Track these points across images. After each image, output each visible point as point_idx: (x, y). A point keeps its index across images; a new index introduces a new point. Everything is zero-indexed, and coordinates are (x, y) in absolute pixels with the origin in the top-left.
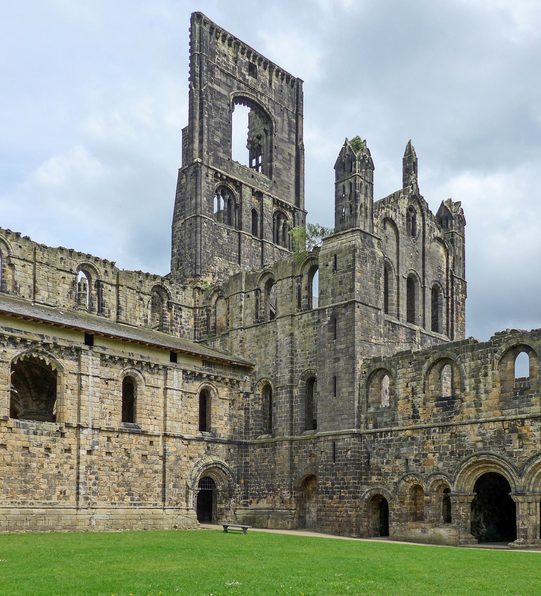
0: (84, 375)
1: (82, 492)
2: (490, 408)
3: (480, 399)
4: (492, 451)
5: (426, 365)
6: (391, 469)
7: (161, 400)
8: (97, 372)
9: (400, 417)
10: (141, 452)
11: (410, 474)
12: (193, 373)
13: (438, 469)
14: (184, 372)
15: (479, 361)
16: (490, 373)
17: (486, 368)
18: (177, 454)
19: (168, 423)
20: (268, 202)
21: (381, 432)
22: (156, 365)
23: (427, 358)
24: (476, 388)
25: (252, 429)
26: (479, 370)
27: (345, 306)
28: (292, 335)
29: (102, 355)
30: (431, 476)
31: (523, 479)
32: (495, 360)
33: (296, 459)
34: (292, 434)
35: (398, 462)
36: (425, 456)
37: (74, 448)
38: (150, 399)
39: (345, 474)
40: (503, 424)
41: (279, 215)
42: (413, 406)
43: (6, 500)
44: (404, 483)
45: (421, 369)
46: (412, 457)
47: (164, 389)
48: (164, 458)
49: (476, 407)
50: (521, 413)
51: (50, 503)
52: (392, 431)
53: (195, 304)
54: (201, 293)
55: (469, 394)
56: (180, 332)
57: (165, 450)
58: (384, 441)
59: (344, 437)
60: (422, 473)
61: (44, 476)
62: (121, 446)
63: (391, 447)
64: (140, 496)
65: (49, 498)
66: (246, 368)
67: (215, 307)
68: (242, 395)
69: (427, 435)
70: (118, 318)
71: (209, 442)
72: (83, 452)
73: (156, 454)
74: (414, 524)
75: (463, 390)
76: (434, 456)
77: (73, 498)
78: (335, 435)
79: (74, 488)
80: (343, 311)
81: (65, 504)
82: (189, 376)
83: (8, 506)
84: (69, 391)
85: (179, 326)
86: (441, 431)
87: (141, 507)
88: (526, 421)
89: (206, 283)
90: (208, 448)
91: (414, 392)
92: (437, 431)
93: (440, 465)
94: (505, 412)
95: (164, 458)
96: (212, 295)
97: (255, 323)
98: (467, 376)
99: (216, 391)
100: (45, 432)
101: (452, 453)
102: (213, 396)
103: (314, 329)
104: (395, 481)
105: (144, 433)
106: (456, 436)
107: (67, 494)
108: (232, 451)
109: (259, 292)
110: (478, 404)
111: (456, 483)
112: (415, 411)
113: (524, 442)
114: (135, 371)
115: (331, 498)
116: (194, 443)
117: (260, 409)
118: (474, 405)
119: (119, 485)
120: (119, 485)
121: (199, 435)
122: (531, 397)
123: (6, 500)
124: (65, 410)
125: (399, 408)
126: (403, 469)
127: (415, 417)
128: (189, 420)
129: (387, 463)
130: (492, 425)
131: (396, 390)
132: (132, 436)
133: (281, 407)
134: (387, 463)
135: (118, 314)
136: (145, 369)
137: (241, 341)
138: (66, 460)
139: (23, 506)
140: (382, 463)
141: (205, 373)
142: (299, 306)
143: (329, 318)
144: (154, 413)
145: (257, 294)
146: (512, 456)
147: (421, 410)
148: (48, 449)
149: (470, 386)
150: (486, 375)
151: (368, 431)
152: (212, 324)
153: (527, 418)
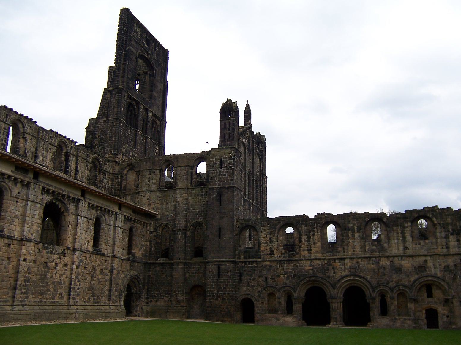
0: (79, 216)
1: (72, 294)
2: (317, 252)
3: (311, 247)
4: (318, 275)
5: (278, 226)
6: (256, 283)
7: (111, 234)
8: (86, 215)
9: (261, 253)
10: (100, 267)
11: (269, 287)
12: (128, 217)
13: (286, 283)
14: (125, 216)
15: (310, 227)
16: (316, 233)
17: (314, 231)
19: (116, 249)
20: (150, 114)
21: (249, 262)
22: (113, 212)
23: (279, 223)
24: (309, 241)
25: (153, 254)
26: (310, 232)
27: (228, 188)
28: (187, 199)
29: (89, 204)
30: (282, 288)
31: (336, 290)
32: (319, 228)
33: (187, 275)
34: (185, 259)
35: (260, 279)
36: (278, 276)
37: (69, 263)
39: (227, 285)
40: (324, 261)
41: (154, 122)
42: (271, 248)
43: (32, 300)
44: (264, 291)
45: (275, 228)
46: (270, 277)
47: (114, 226)
48: (111, 272)
49: (308, 251)
50: (333, 256)
51: (55, 302)
52: (256, 262)
53: (113, 171)
54: (117, 165)
55: (304, 244)
56: (104, 188)
57: (112, 266)
58: (251, 267)
59: (226, 263)
60: (276, 286)
61: (53, 283)
62: (91, 263)
63: (256, 271)
64: (98, 296)
65: (54, 298)
66: (151, 216)
67: (126, 175)
68: (148, 232)
69: (279, 265)
70: (75, 177)
71: (132, 261)
72: (75, 267)
74: (271, 315)
75: (301, 241)
76: (284, 276)
77: (65, 298)
78: (219, 262)
79: (67, 290)
80: (226, 191)
81: (62, 302)
82: (127, 219)
83: (33, 304)
84: (70, 226)
85: (104, 184)
86: (288, 263)
87: (98, 304)
88: (336, 261)
89: (119, 159)
91: (271, 241)
92: (286, 263)
93: (288, 282)
94: (325, 255)
95: (111, 272)
96: (126, 168)
97: (158, 189)
98: (303, 234)
100: (56, 253)
101: (295, 275)
103: (202, 198)
104: (259, 290)
105: (103, 255)
106: (297, 266)
107: (63, 295)
109: (162, 171)
110: (310, 250)
111: (297, 292)
112: (272, 251)
113: (336, 271)
114: (101, 214)
115: (216, 299)
118: (307, 250)
119: (88, 290)
120: (88, 290)
122: (338, 248)
123: (32, 300)
124: (67, 238)
125: (261, 249)
126: (264, 283)
127: (272, 253)
129: (254, 280)
130: (318, 262)
131: (260, 238)
132: (97, 256)
133: (178, 242)
134: (254, 280)
135: (76, 174)
136: (106, 213)
137: (148, 199)
138: (64, 272)
139: (41, 304)
140: (250, 280)
141: (134, 218)
142: (191, 183)
143: (217, 194)
145: (160, 172)
146: (329, 278)
147: (275, 251)
148: (56, 264)
149: (305, 240)
150: (314, 235)
151: (241, 260)
152: (123, 186)
153: (337, 259)
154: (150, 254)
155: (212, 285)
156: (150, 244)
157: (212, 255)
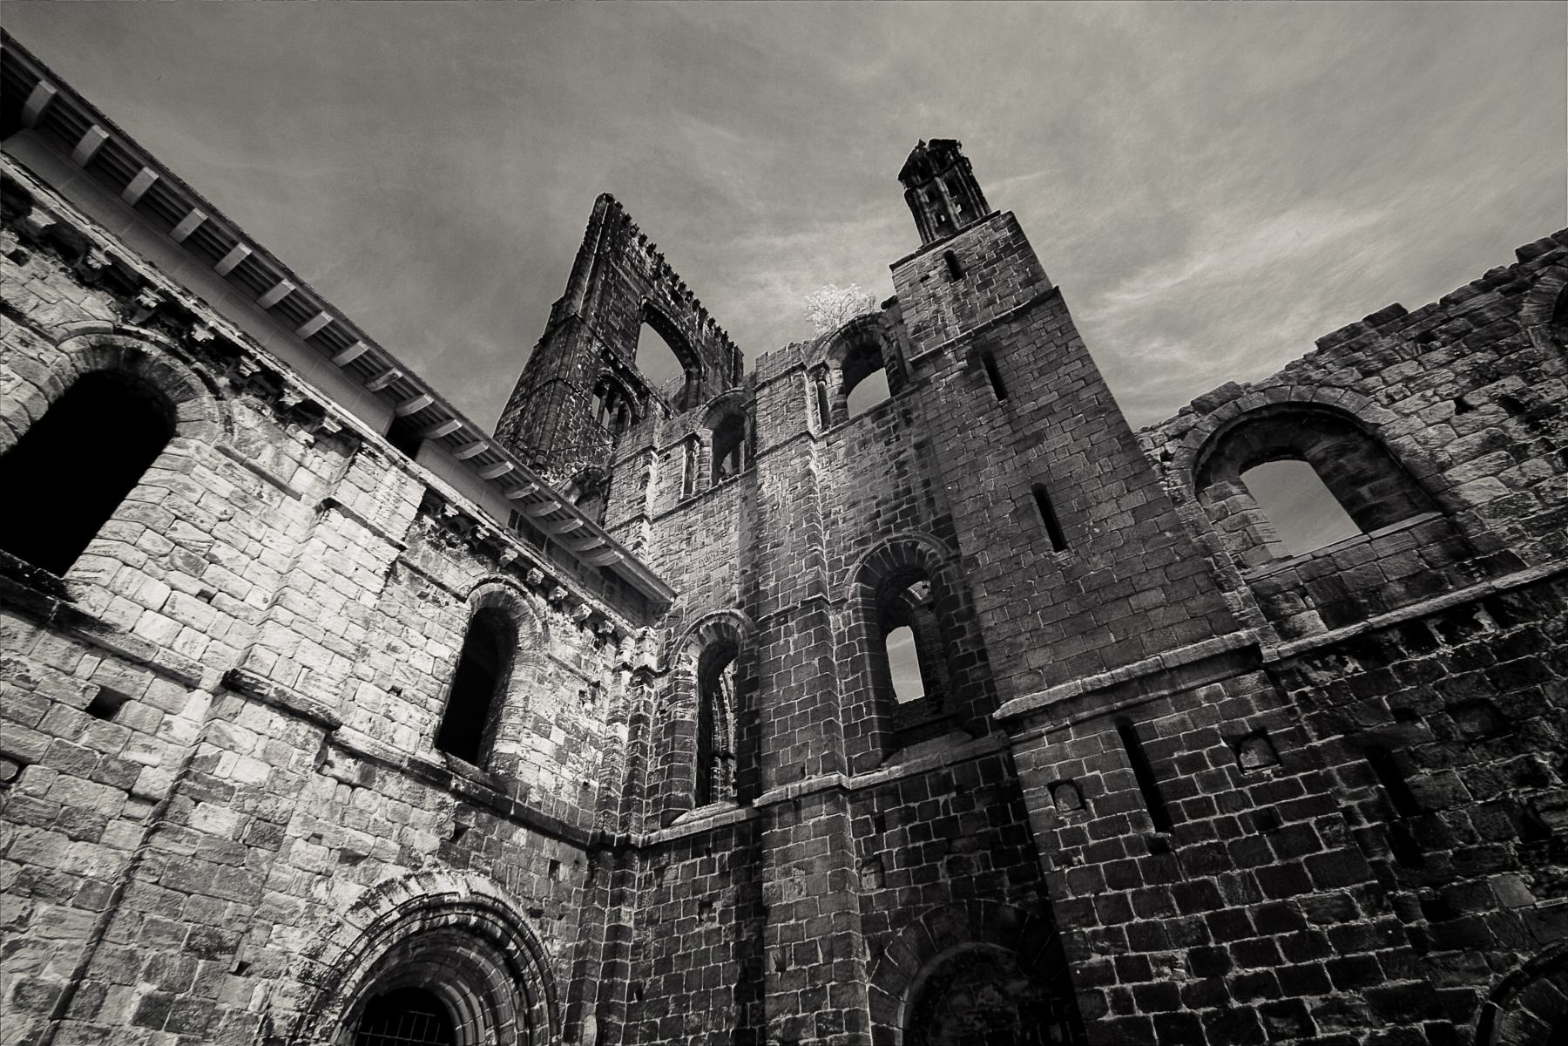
14: (432, 502)
18: (266, 806)
38: (218, 507)
39: (1289, 880)
68: (626, 675)
73: (126, 779)
78: (1117, 688)
90: (459, 832)
99: (539, 628)
102: (525, 641)
108: (564, 871)
116: (394, 785)
117: (687, 718)
121: (434, 758)
128: (397, 679)
144: (212, 569)
154: (629, 791)
155: (1118, 909)
156: (633, 734)
157: (1038, 658)
